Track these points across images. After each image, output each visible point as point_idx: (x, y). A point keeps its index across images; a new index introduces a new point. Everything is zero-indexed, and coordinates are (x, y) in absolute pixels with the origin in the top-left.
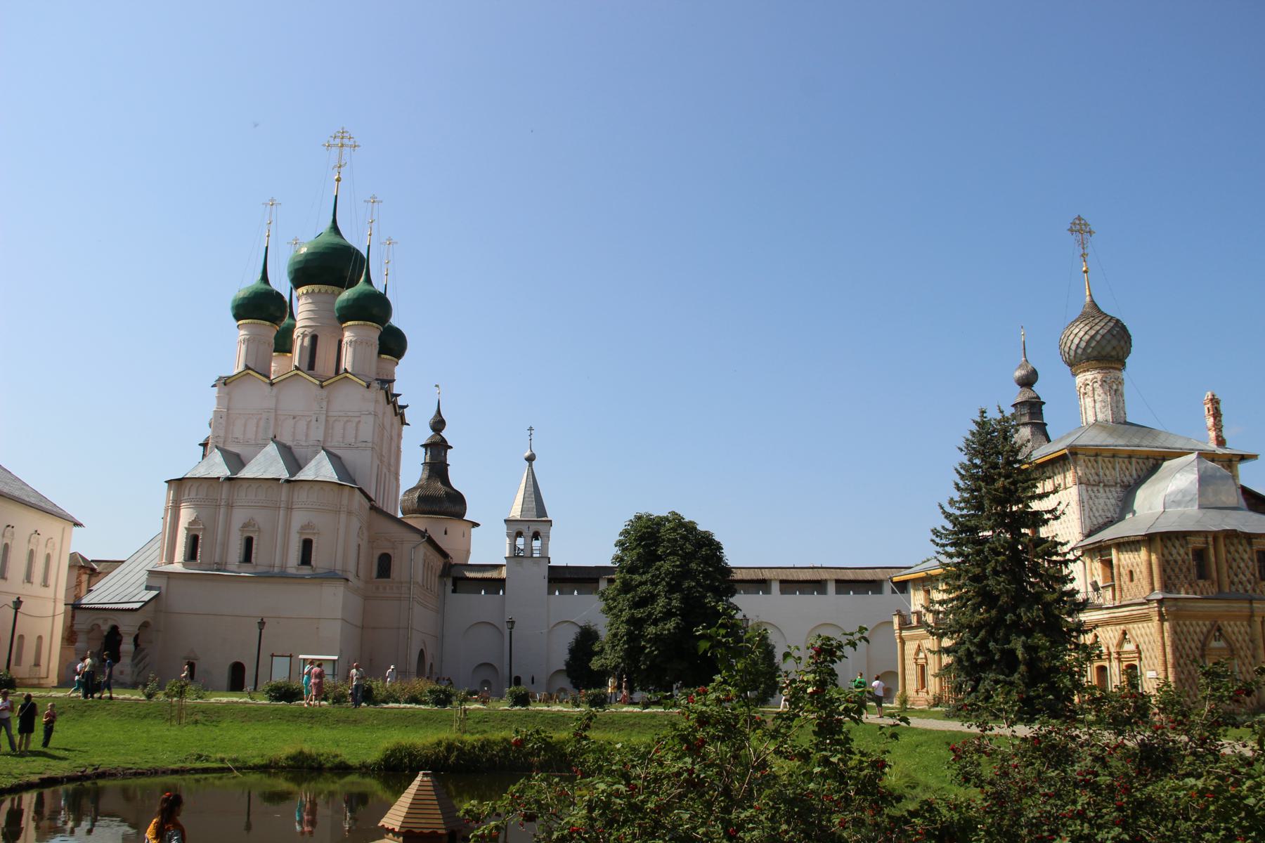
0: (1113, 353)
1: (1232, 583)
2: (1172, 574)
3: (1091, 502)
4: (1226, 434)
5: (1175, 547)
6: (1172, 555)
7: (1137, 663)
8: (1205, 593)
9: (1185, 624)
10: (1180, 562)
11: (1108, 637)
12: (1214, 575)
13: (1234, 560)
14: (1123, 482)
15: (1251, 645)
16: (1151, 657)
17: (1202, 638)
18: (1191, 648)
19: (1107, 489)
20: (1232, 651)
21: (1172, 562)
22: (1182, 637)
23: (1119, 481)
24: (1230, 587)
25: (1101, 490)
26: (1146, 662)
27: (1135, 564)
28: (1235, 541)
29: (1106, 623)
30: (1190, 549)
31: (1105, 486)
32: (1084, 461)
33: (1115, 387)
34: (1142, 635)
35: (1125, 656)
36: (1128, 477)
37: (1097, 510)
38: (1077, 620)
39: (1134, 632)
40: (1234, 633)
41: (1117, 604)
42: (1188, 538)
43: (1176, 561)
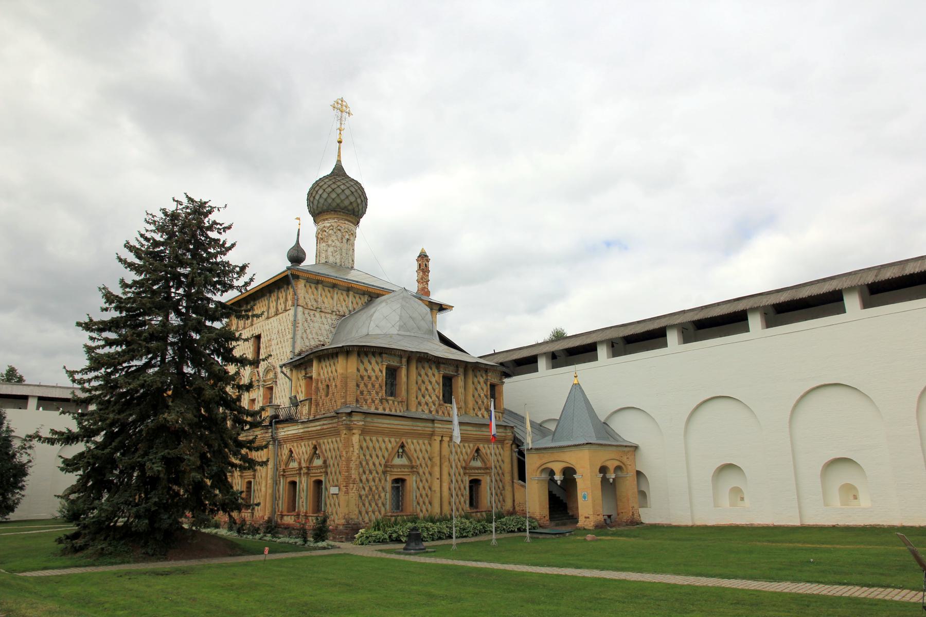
0: (350, 208)
1: (419, 403)
2: (365, 389)
3: (306, 325)
4: (430, 287)
5: (371, 364)
6: (366, 370)
7: (323, 479)
8: (393, 410)
9: (371, 440)
10: (373, 378)
11: (301, 452)
12: (404, 393)
13: (423, 382)
14: (339, 312)
15: (429, 463)
16: (336, 473)
17: (386, 455)
18: (374, 464)
19: (323, 315)
20: (413, 469)
21: (366, 378)
22: (367, 453)
23: (335, 309)
24: (417, 407)
25: (318, 315)
26: (331, 478)
27: (332, 379)
28: (426, 365)
29: (299, 438)
30: (385, 366)
31: (321, 311)
32: (305, 286)
33: (347, 237)
34: (330, 450)
35: (314, 471)
36: (344, 309)
37: (311, 332)
38: (139, 389)
39: (323, 447)
40: (415, 451)
41: (311, 419)
42: (383, 355)
43: (369, 377)
